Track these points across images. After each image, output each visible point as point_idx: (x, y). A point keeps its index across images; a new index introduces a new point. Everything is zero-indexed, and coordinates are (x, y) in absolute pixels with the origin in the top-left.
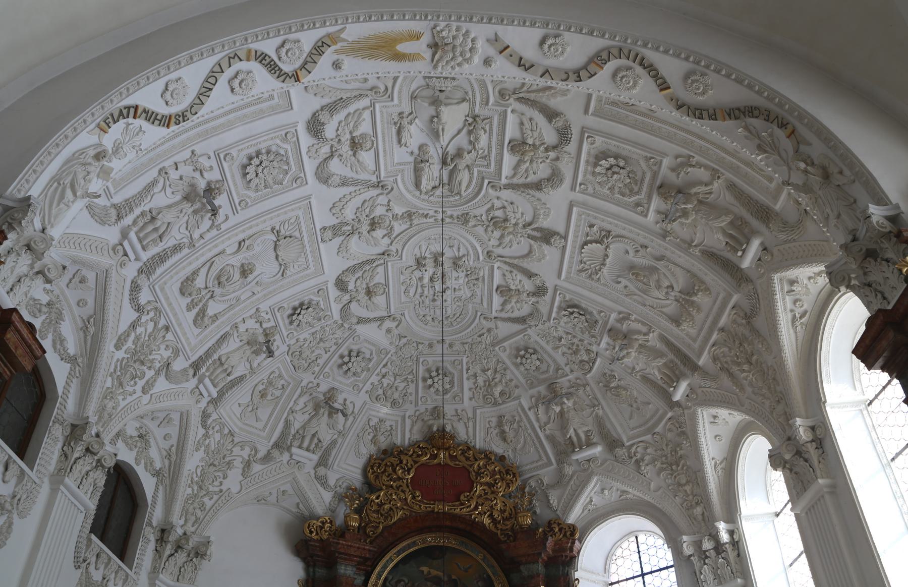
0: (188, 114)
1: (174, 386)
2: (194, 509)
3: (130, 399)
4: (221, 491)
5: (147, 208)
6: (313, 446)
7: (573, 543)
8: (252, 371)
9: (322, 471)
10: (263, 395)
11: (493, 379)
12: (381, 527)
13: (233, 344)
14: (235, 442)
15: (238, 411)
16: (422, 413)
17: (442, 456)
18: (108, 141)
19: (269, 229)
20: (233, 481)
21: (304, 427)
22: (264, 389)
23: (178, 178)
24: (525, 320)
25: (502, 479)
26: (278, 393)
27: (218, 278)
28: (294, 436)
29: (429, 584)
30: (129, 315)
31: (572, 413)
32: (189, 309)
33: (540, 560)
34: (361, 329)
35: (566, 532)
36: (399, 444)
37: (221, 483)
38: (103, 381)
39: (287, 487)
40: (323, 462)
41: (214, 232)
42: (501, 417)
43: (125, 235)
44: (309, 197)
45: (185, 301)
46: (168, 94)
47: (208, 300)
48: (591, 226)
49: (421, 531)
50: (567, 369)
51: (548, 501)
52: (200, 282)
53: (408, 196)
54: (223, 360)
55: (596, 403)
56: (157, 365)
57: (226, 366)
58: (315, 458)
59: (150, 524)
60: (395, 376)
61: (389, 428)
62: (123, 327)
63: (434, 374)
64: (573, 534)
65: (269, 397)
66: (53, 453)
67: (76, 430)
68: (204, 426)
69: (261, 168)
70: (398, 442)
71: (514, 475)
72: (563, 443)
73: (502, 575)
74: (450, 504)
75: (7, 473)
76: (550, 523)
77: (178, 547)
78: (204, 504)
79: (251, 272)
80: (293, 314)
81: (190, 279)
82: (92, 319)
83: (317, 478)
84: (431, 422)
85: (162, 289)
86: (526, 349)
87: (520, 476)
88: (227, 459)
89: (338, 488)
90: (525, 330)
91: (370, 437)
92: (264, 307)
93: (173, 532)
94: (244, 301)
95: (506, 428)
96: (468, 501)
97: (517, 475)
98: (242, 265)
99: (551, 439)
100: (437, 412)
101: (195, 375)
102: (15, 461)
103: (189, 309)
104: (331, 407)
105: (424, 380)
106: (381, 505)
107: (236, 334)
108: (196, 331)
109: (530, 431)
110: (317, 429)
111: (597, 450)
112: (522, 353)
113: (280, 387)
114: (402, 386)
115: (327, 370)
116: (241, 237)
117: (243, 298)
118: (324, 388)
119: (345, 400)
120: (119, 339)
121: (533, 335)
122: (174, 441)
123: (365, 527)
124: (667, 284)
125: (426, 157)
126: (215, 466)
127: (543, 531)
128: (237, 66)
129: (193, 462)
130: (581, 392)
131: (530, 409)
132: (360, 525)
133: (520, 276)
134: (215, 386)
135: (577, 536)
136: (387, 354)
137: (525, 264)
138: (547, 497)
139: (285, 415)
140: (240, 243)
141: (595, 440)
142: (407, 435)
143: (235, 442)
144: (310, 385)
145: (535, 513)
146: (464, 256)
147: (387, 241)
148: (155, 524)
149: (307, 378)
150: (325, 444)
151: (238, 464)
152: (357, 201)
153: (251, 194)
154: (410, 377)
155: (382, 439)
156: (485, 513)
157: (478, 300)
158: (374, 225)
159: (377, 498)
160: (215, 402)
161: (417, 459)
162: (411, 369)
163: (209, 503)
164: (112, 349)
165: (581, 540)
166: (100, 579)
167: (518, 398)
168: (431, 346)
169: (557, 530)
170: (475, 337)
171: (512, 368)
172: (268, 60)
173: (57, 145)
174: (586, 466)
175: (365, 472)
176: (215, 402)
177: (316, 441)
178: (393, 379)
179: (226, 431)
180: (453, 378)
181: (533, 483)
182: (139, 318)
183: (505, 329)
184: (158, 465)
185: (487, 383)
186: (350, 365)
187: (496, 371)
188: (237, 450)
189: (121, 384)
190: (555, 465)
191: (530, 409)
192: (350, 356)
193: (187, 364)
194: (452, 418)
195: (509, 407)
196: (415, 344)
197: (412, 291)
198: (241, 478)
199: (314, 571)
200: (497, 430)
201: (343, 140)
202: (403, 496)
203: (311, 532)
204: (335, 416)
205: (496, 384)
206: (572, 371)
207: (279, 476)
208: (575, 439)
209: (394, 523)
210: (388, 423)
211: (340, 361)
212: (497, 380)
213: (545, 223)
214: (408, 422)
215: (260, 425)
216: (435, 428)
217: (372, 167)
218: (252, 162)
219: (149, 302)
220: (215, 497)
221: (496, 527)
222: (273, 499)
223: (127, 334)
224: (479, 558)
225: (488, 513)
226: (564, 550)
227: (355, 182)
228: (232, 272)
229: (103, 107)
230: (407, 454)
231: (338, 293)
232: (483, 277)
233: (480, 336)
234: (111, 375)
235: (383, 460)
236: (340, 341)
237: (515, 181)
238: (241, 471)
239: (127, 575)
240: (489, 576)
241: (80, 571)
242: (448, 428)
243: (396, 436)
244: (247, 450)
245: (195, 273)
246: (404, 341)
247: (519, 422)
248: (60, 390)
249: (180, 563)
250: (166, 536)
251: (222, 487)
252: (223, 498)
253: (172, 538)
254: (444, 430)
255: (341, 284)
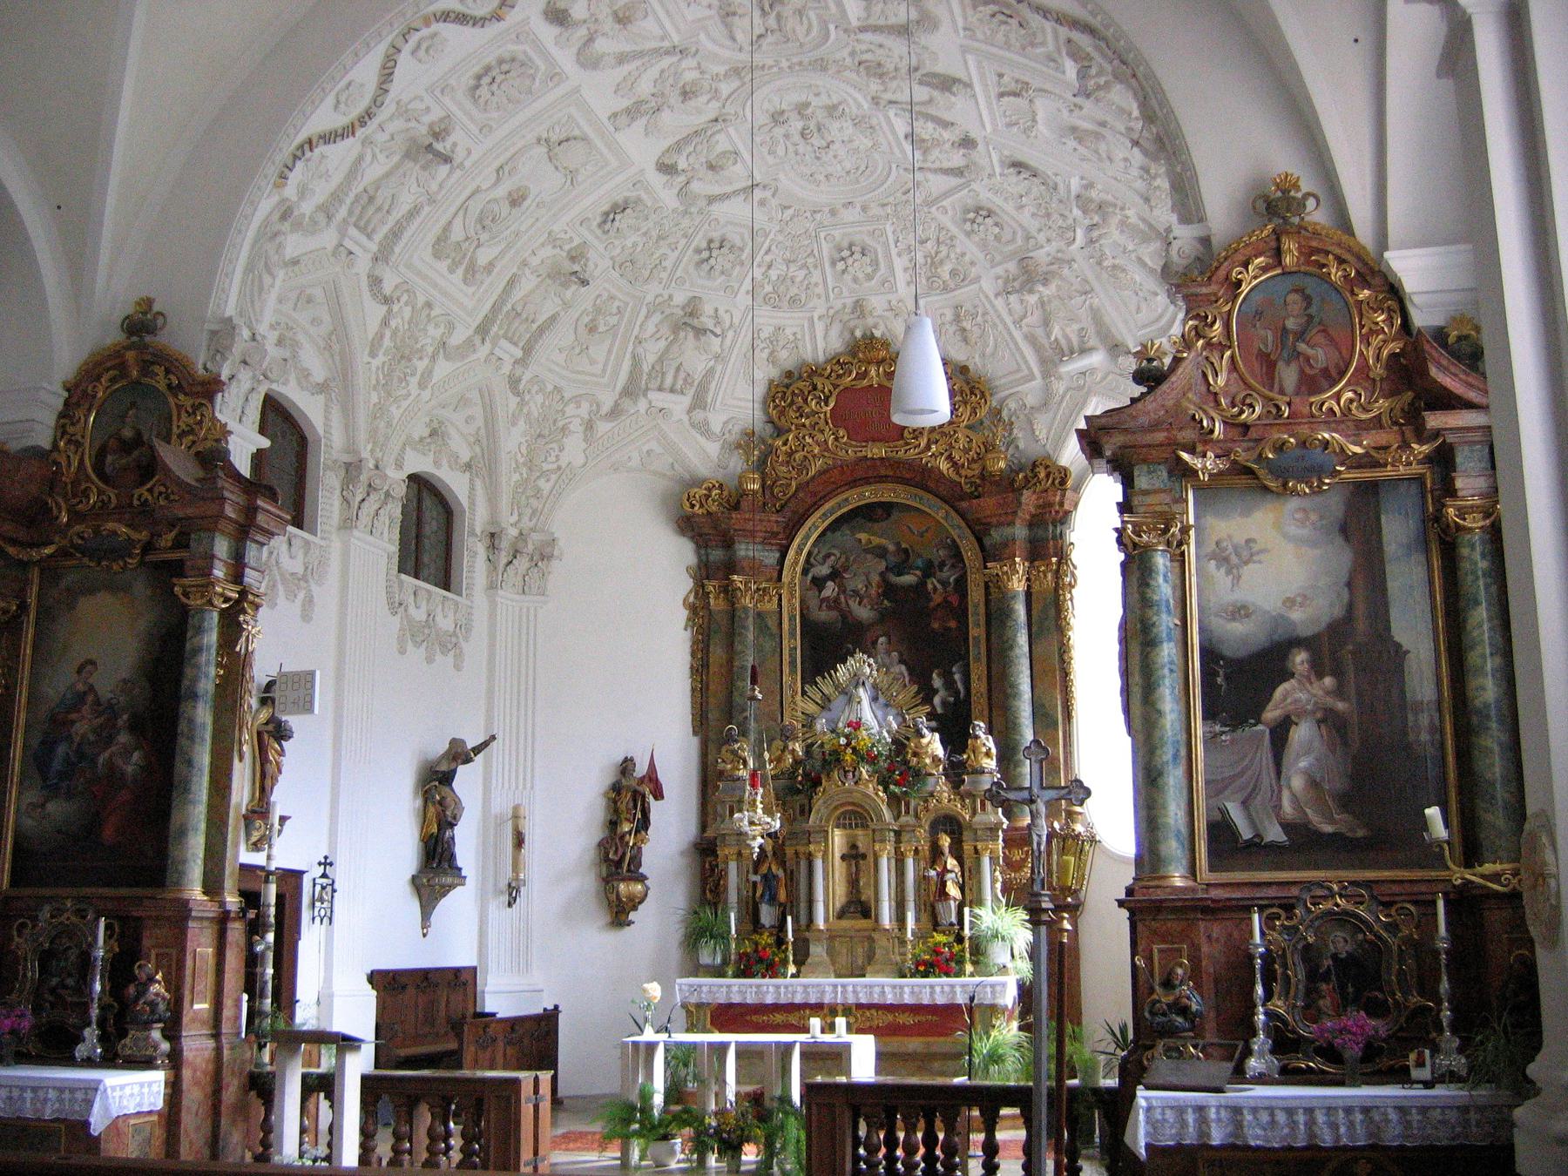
0: (374, 109)
1: (460, 364)
2: (527, 498)
3: (405, 404)
4: (559, 468)
5: (361, 188)
6: (680, 382)
7: (1063, 496)
8: (567, 305)
9: (699, 415)
10: (592, 329)
11: (937, 253)
12: (794, 484)
13: (527, 284)
14: (566, 399)
15: (561, 359)
16: (837, 312)
17: (873, 373)
18: (290, 191)
19: (534, 141)
20: (574, 449)
21: (661, 360)
22: (592, 321)
23: (388, 137)
24: (962, 173)
25: (965, 403)
26: (613, 320)
27: (480, 220)
28: (649, 375)
29: (869, 556)
30: (376, 311)
31: (1056, 303)
32: (451, 271)
33: (1018, 522)
34: (718, 209)
35: (1054, 479)
36: (810, 361)
37: (558, 460)
38: (367, 398)
39: (653, 445)
40: (699, 403)
41: (458, 173)
42: (957, 307)
43: (343, 233)
44: (577, 90)
45: (443, 266)
46: (342, 106)
47: (474, 252)
48: (1001, 76)
49: (853, 483)
50: (1041, 238)
51: (1033, 431)
52: (457, 234)
53: (727, 54)
54: (519, 309)
55: (1088, 289)
56: (430, 350)
57: (524, 316)
58: (686, 400)
59: (472, 533)
60: (788, 262)
61: (791, 338)
62: (373, 326)
63: (846, 253)
64: (1063, 482)
65: (602, 329)
66: (332, 505)
67: (351, 469)
68: (518, 394)
69: (495, 87)
70: (808, 355)
71: (983, 395)
72: (1047, 346)
73: (972, 538)
74: (891, 444)
75: (293, 549)
76: (1034, 465)
77: (516, 553)
78: (539, 490)
79: (524, 200)
80: (605, 222)
81: (442, 239)
82: (333, 337)
83: (693, 425)
84: (852, 324)
85: (409, 266)
86: (977, 210)
87: (991, 395)
88: (560, 424)
89: (727, 436)
90: (967, 184)
91: (765, 355)
92: (556, 228)
93: (504, 537)
94: (526, 231)
95: (967, 325)
96: (916, 438)
97: (987, 394)
98: (510, 194)
99: (1031, 339)
100: (859, 307)
101: (483, 340)
102: (295, 536)
103: (451, 271)
104: (693, 328)
105: (833, 264)
106: (791, 454)
107: (527, 271)
108: (471, 290)
109: (1000, 327)
110: (679, 361)
111: (1097, 359)
112: (972, 215)
113: (614, 310)
114: (801, 274)
115: (678, 274)
116: (497, 164)
117: (523, 228)
118: (680, 298)
119: (716, 310)
120: (372, 345)
121: (982, 192)
122: (480, 422)
123: (771, 487)
124: (1121, 156)
125: (732, 9)
126: (544, 437)
127: (1026, 477)
128: (414, 38)
129: (513, 440)
130: (1066, 271)
131: (997, 295)
132: (763, 486)
133: (930, 125)
134: (515, 344)
135: (1070, 483)
136: (766, 236)
137: (932, 111)
138: (1031, 424)
139: (630, 349)
140: (498, 172)
141: (1091, 343)
142: (821, 345)
143: (566, 399)
144: (660, 299)
145: (1017, 447)
146: (840, 104)
147: (715, 105)
148: (478, 531)
149: (653, 290)
150: (698, 378)
151: (576, 426)
152: (653, 72)
153: (495, 115)
154: (810, 260)
155: (783, 354)
156: (942, 454)
157: (885, 147)
158: (686, 94)
159: (785, 444)
160: (521, 362)
161: (838, 382)
162: (809, 251)
163: (545, 486)
164: (366, 359)
165: (1077, 489)
166: (424, 617)
167: (977, 279)
168: (833, 212)
169: (1042, 475)
170: (899, 195)
171: (961, 236)
172: (452, 15)
173: (240, 231)
174: (1081, 382)
175: (765, 403)
176: (521, 362)
177: (682, 375)
178: (784, 268)
179: (550, 388)
180: (877, 256)
181: (1012, 405)
182: (390, 311)
183: (938, 183)
184: (465, 456)
185: (929, 260)
186: (712, 261)
187: (938, 242)
188: (570, 410)
189: (389, 394)
190: (1038, 382)
191: (997, 295)
192: (710, 249)
193: (470, 332)
194: (886, 314)
195: (964, 294)
196: (808, 214)
197: (780, 151)
198: (584, 445)
199: (707, 555)
200: (954, 328)
201: (601, 17)
202: (821, 438)
203: (693, 506)
204: (703, 339)
205: (941, 262)
206: (1048, 240)
207: (637, 434)
208: (1063, 342)
209: (813, 477)
210: (788, 331)
211: (697, 258)
212: (944, 254)
213: (940, 68)
214: (820, 327)
215: (598, 368)
216: (858, 334)
217: (658, 32)
218: (482, 82)
219: (396, 287)
220: (554, 477)
221: (958, 473)
222: (635, 462)
223: (380, 336)
224: (940, 516)
225: (946, 454)
226: (1051, 505)
227: (639, 55)
228: (496, 209)
229: (273, 163)
230: (821, 375)
231: (665, 178)
232: (879, 124)
233: (905, 193)
234: (375, 388)
235: (787, 386)
236: (691, 231)
237: (871, 21)
238: (581, 436)
239: (457, 604)
240: (954, 541)
241: (397, 619)
242: (877, 334)
243: (805, 346)
244: (585, 406)
245: (447, 228)
246: (790, 212)
247: (984, 314)
248: (321, 431)
249: (522, 570)
250: (496, 542)
251: (559, 463)
252: (564, 477)
253: (505, 544)
254: (872, 337)
255: (667, 168)
